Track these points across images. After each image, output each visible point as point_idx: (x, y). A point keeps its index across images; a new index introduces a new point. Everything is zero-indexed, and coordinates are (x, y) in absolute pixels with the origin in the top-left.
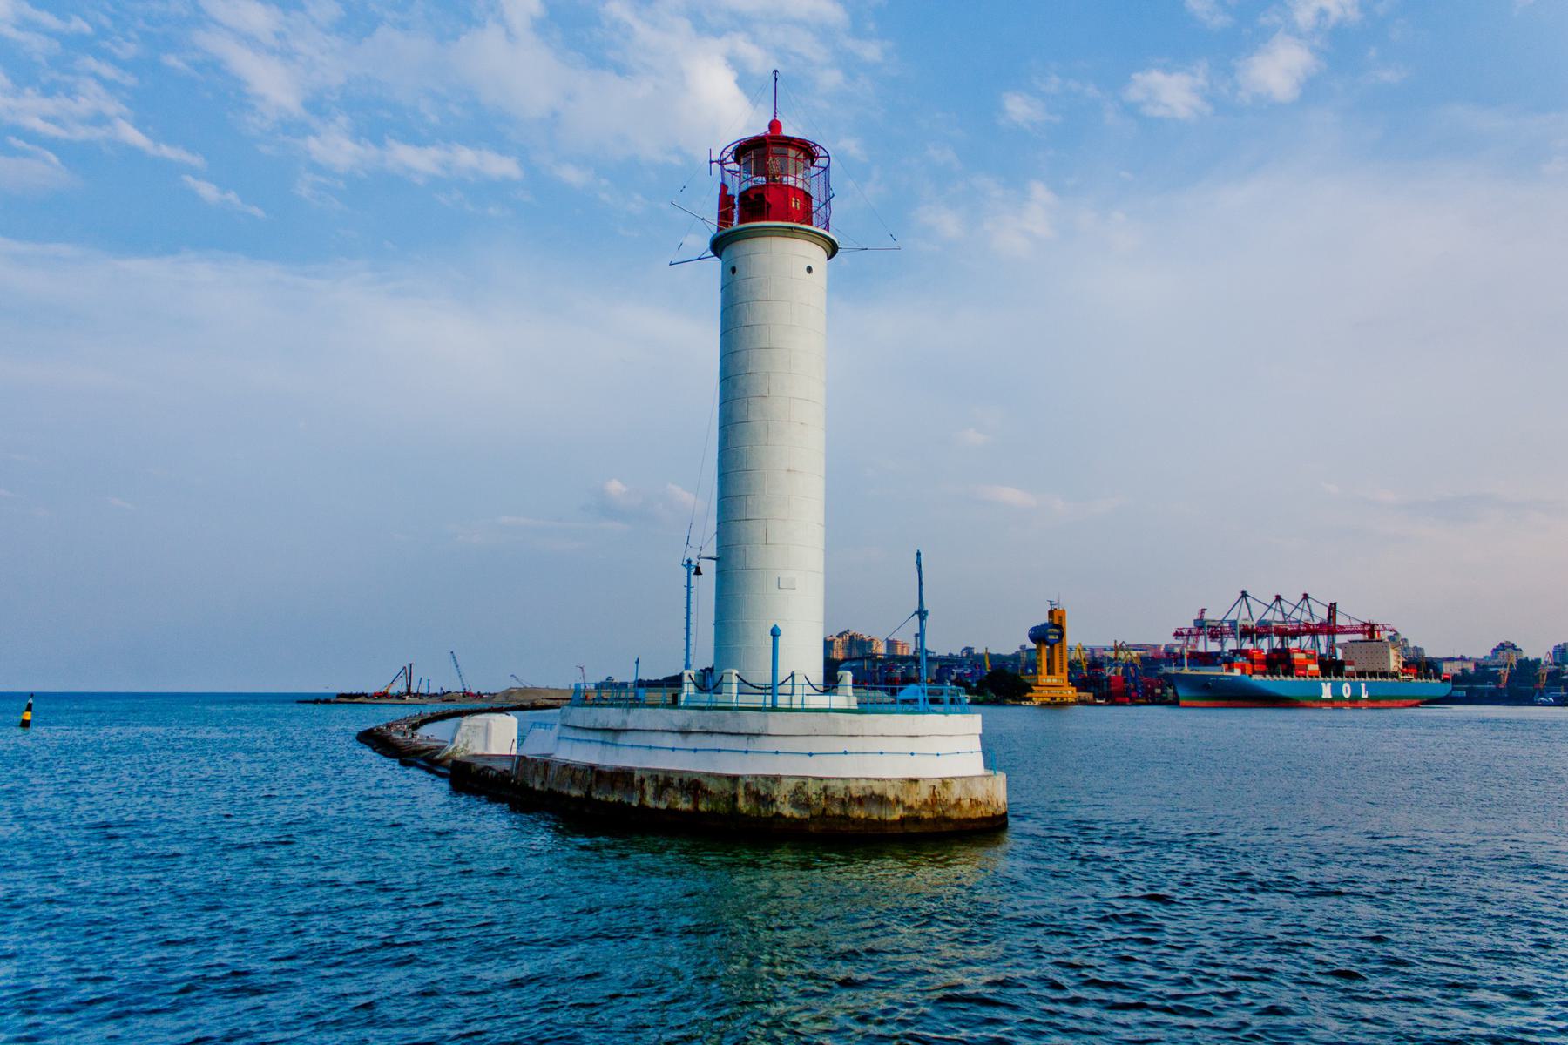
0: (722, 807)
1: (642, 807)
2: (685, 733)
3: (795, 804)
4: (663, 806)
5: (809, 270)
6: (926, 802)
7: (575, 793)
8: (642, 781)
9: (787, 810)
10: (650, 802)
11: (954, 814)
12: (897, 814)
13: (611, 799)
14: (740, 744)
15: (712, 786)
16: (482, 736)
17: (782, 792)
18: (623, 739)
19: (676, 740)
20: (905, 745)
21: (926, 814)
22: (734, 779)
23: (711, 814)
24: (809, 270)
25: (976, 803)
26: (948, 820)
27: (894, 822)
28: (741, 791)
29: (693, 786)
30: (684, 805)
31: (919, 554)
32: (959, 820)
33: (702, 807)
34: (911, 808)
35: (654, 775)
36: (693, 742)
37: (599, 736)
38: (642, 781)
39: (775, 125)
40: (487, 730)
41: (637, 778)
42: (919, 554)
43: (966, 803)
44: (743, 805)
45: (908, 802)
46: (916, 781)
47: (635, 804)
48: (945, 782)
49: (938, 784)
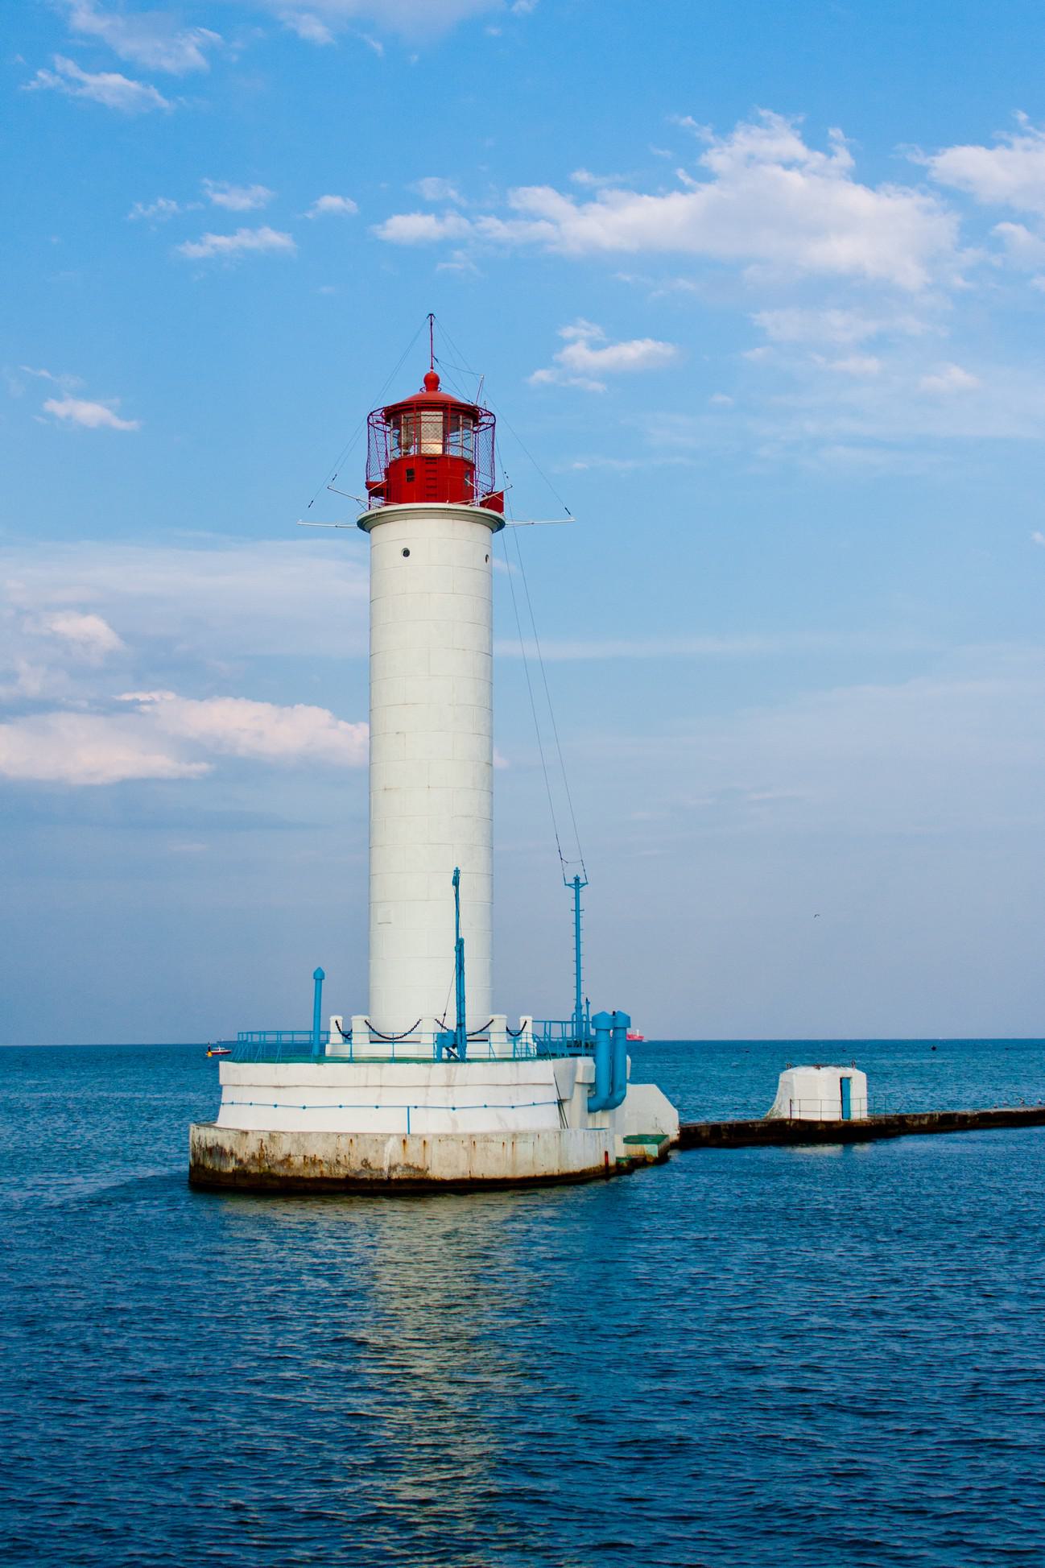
5: (406, 553)
6: (253, 1157)
11: (281, 1171)
12: (231, 1166)
20: (271, 1096)
21: (254, 1169)
24: (406, 553)
25: (315, 1162)
26: (273, 1176)
27: (228, 1175)
31: (457, 872)
32: (286, 1178)
34: (240, 1161)
39: (432, 382)
42: (457, 872)
43: (298, 1161)
45: (240, 1156)
46: (246, 1133)
48: (272, 1136)
49: (265, 1137)
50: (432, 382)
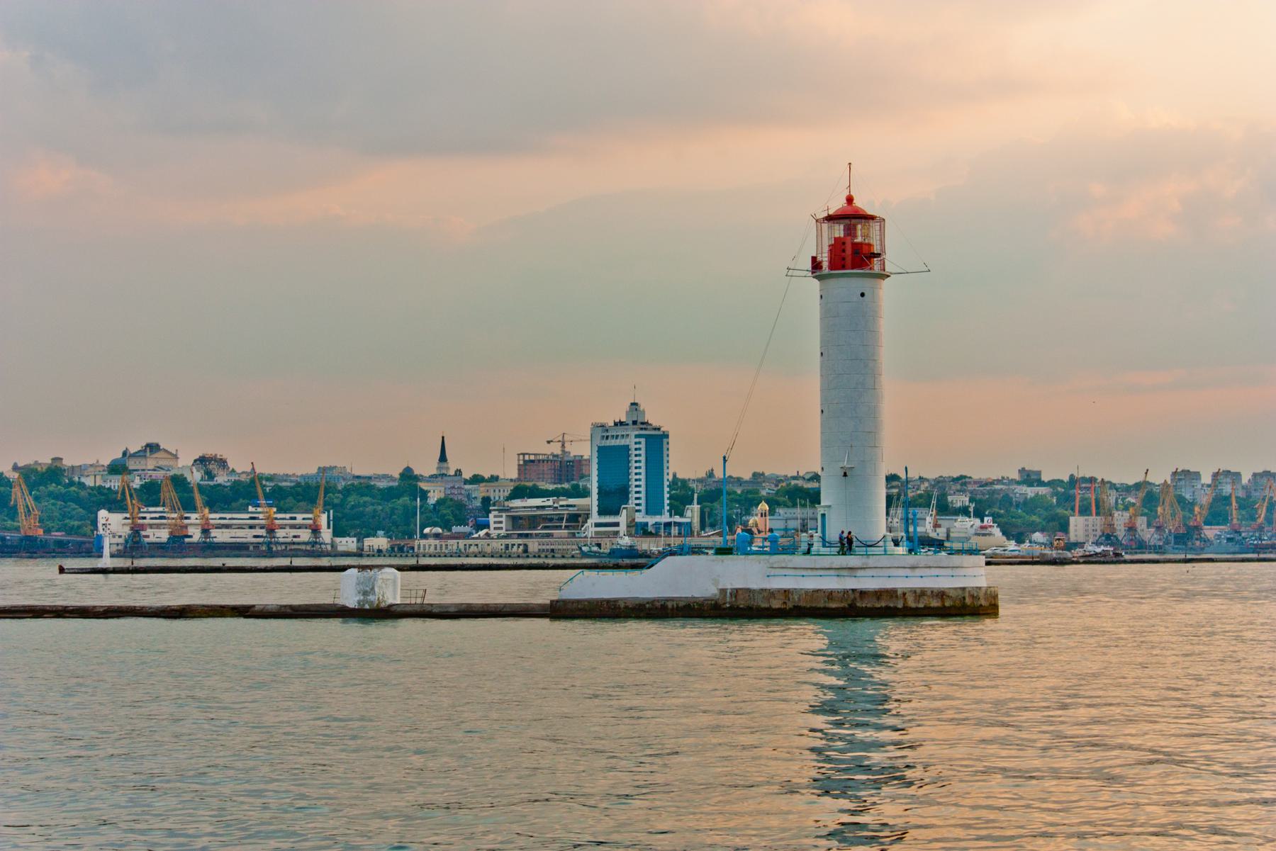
0: (958, 603)
1: (906, 608)
2: (913, 568)
3: (986, 599)
4: (921, 605)
7: (833, 605)
8: (904, 594)
9: (983, 602)
10: (911, 604)
13: (878, 605)
14: (949, 572)
15: (952, 594)
16: (391, 588)
17: (981, 594)
18: (860, 573)
19: (908, 572)
22: (964, 589)
23: (949, 608)
28: (967, 595)
29: (941, 594)
30: (935, 603)
33: (947, 604)
35: (914, 591)
36: (918, 572)
37: (832, 572)
38: (904, 594)
39: (850, 200)
40: (395, 582)
41: (899, 592)
44: (968, 601)
47: (900, 605)
50: (850, 200)
